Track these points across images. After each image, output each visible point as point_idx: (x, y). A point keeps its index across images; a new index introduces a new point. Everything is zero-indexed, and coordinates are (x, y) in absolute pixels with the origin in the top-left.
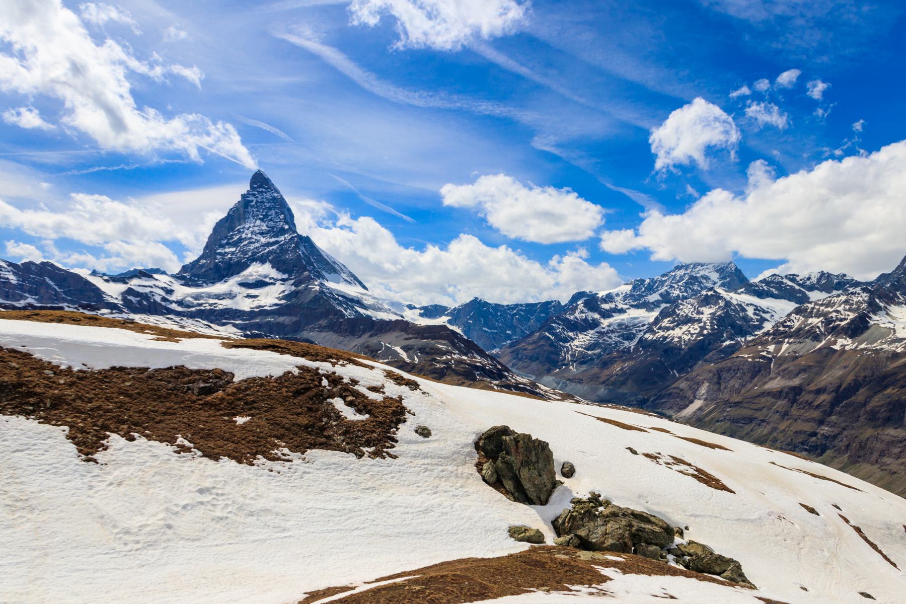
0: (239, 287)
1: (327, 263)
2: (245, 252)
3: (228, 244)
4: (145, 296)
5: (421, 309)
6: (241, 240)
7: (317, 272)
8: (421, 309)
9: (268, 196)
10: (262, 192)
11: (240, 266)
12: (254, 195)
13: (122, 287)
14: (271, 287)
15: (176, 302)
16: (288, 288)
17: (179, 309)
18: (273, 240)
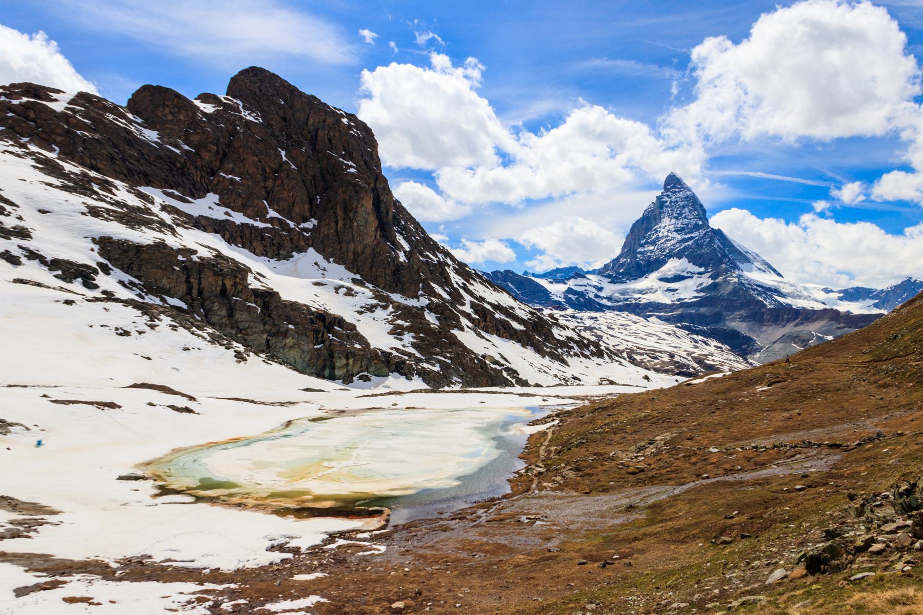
0: (659, 282)
1: (740, 253)
2: (662, 250)
3: (646, 243)
4: (581, 294)
5: (839, 292)
6: (658, 238)
7: (732, 263)
8: (839, 292)
9: (681, 195)
10: (675, 192)
11: (657, 264)
12: (668, 196)
13: (562, 288)
14: (689, 280)
15: (606, 298)
16: (707, 281)
17: (609, 304)
18: (689, 236)
